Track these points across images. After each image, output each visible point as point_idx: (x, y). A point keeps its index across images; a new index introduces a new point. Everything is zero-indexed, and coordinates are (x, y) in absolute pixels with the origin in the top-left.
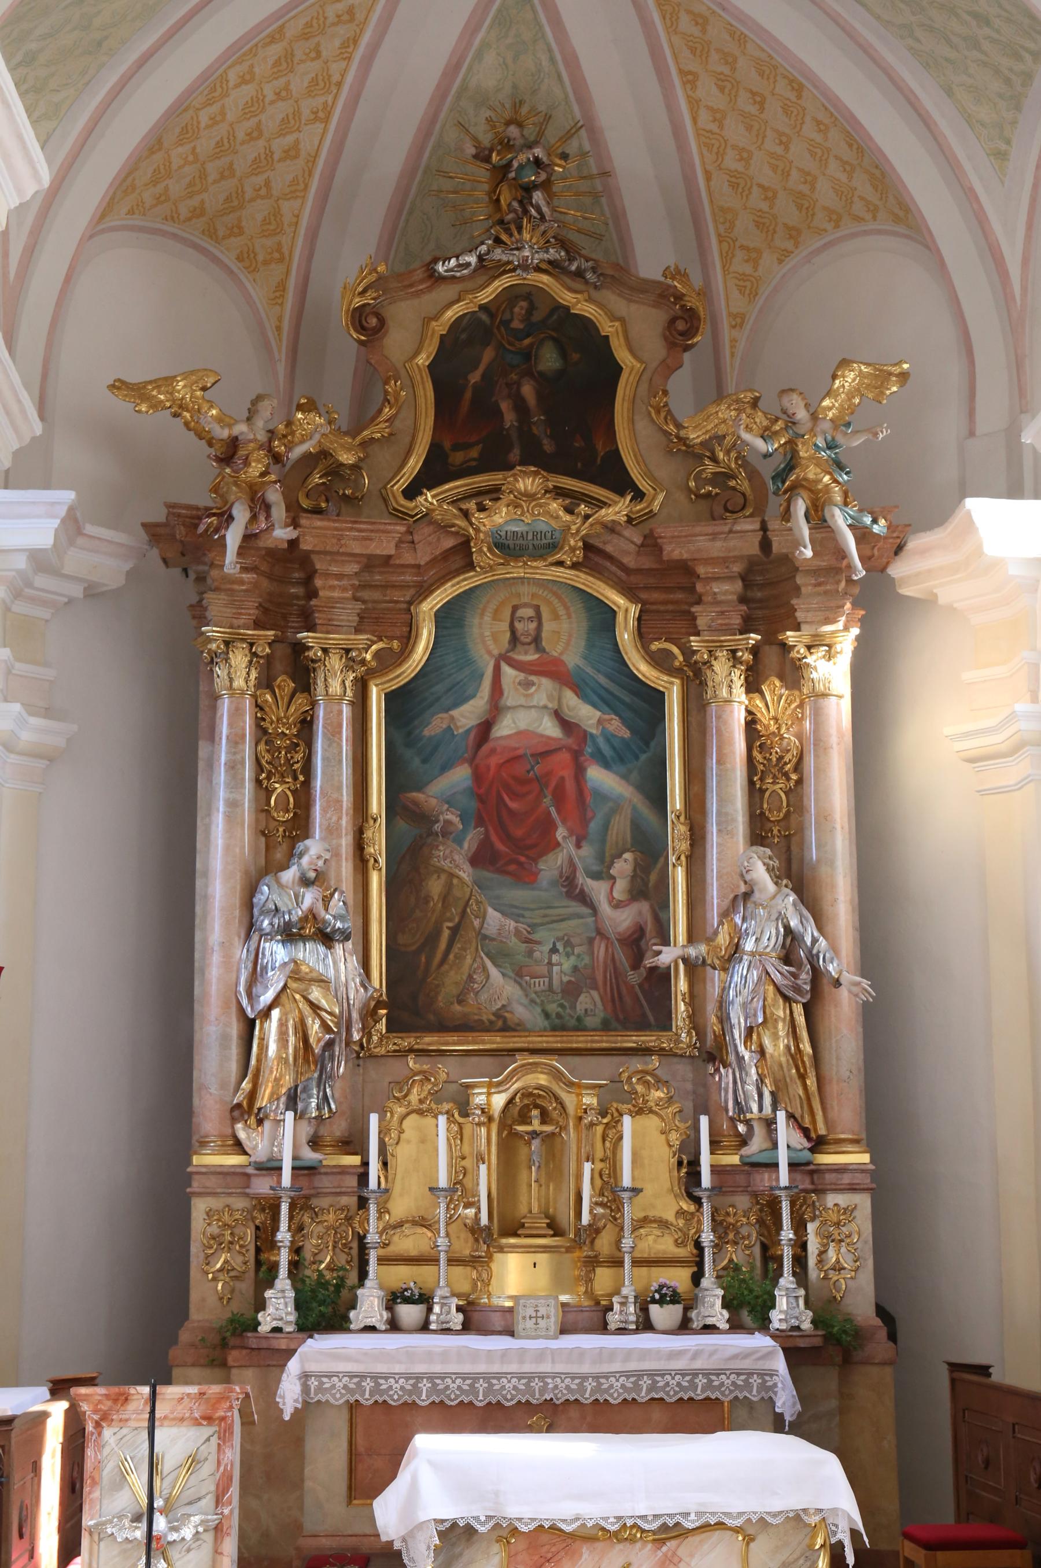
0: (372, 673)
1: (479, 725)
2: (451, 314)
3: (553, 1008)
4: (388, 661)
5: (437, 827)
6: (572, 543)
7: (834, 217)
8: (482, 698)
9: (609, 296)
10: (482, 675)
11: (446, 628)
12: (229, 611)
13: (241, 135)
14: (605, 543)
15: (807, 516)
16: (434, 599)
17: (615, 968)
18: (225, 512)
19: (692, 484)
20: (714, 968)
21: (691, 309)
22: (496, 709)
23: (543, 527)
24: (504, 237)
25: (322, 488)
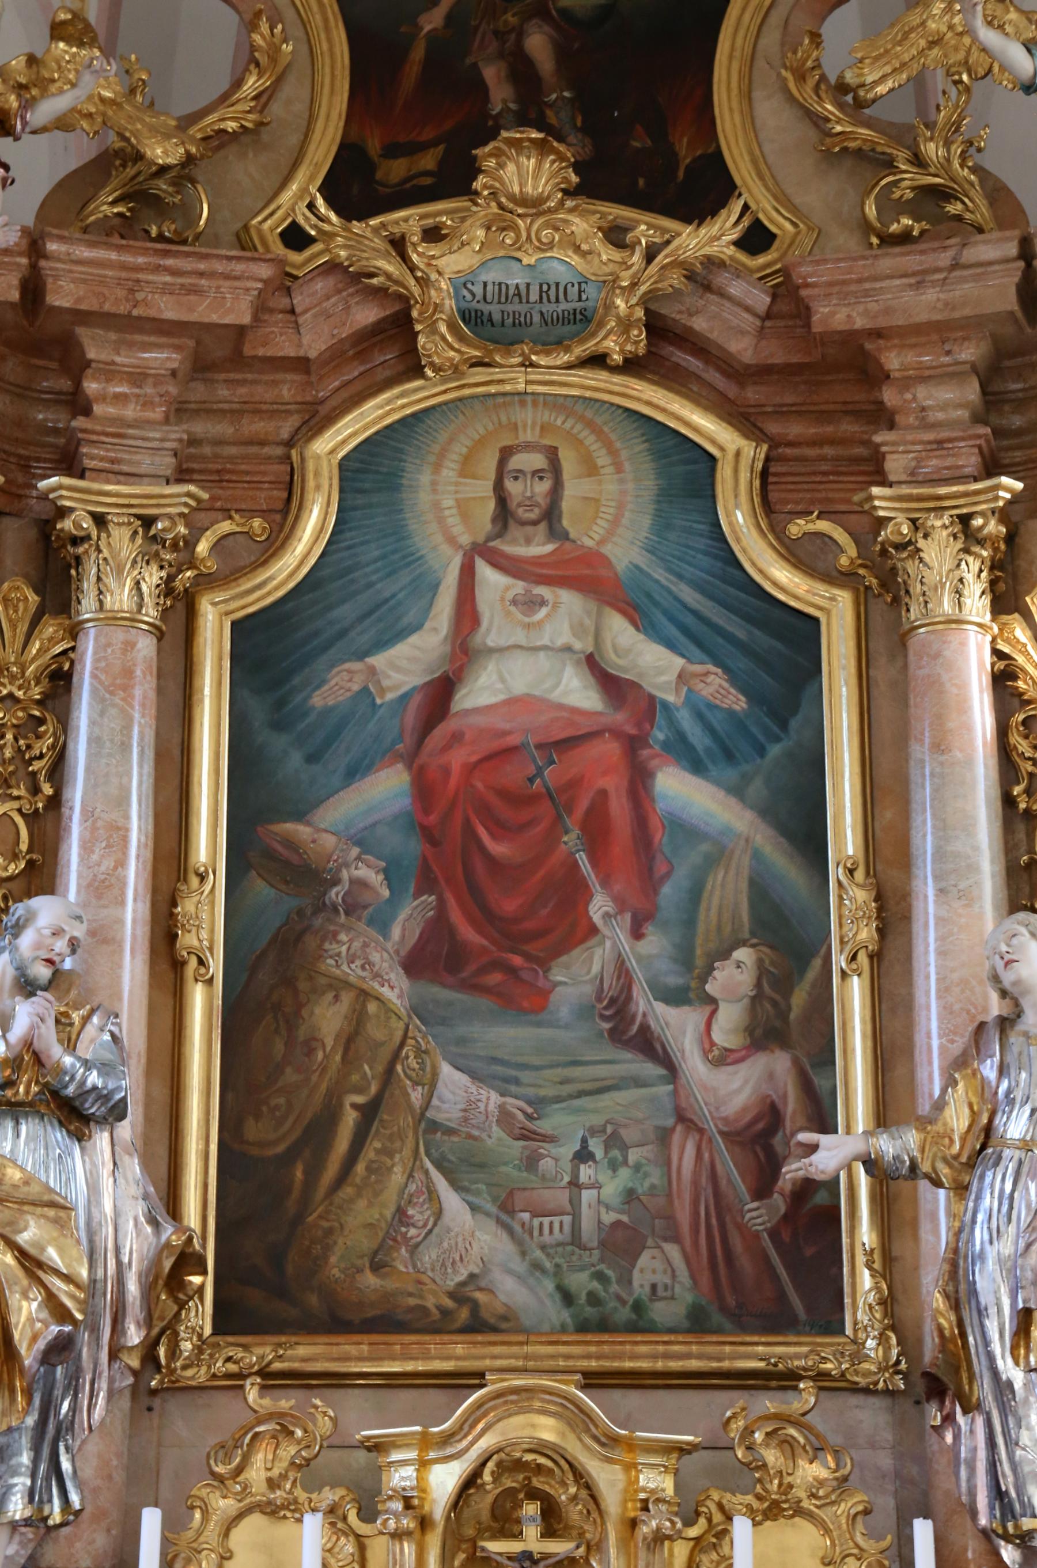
0: (207, 581)
1: (427, 684)
3: (580, 1281)
5: (335, 894)
8: (435, 630)
10: (435, 587)
14: (691, 315)
16: (338, 432)
19: (871, 210)
20: (937, 1183)
25: (117, 221)
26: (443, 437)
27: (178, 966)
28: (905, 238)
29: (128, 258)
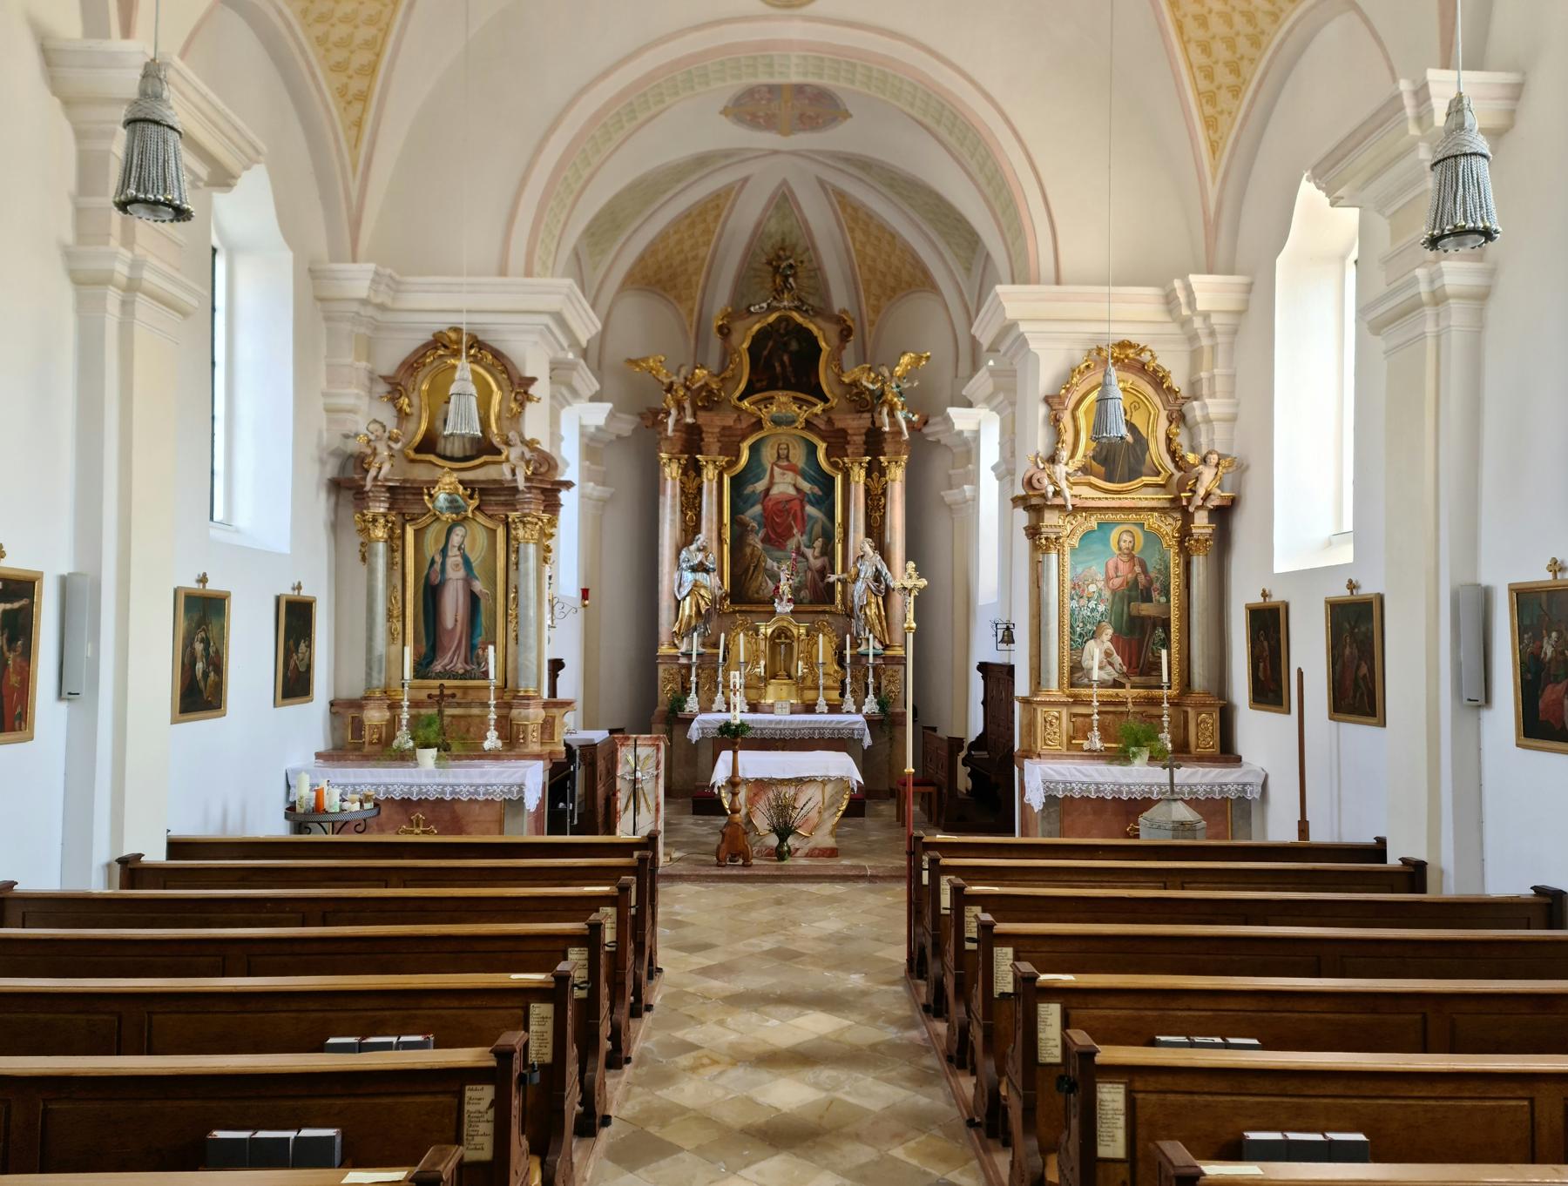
2: (757, 327)
4: (731, 464)
9: (819, 320)
22: (771, 483)
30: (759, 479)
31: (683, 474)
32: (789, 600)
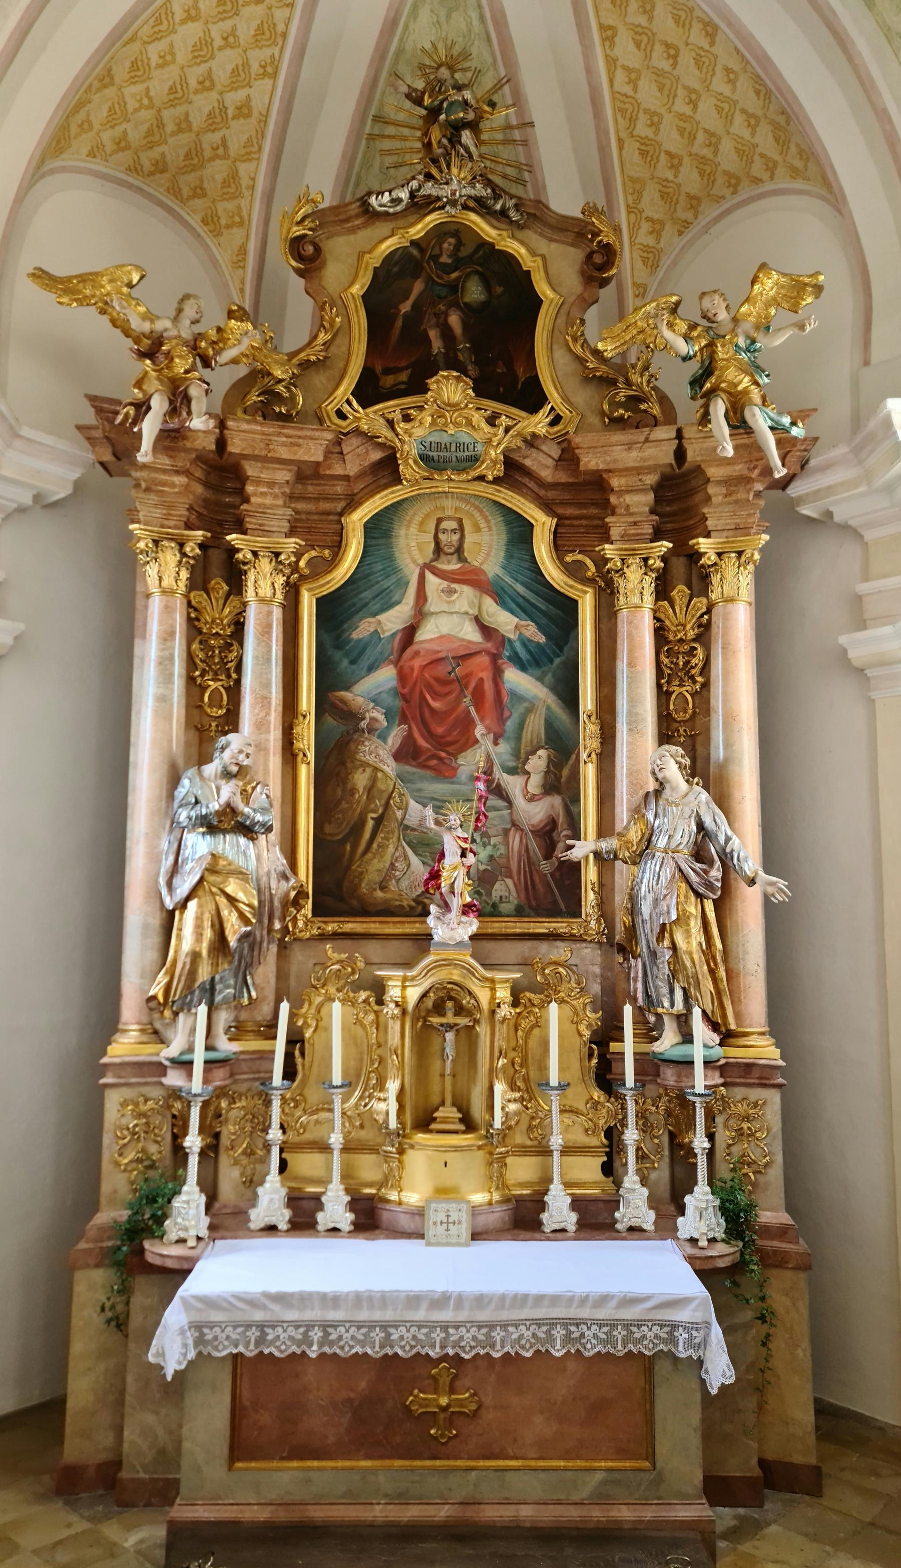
0: (303, 578)
5: (363, 724)
6: (492, 453)
7: (733, 181)
9: (531, 236)
11: (374, 538)
12: (158, 513)
13: (193, 83)
15: (726, 415)
17: (529, 858)
18: (144, 403)
19: (606, 407)
21: (608, 244)
22: (420, 614)
23: (465, 439)
24: (434, 171)
25: (260, 405)
26: (411, 512)
27: (294, 756)
28: (621, 419)
29: (265, 429)
30: (388, 606)
31: (192, 585)
32: (467, 909)
